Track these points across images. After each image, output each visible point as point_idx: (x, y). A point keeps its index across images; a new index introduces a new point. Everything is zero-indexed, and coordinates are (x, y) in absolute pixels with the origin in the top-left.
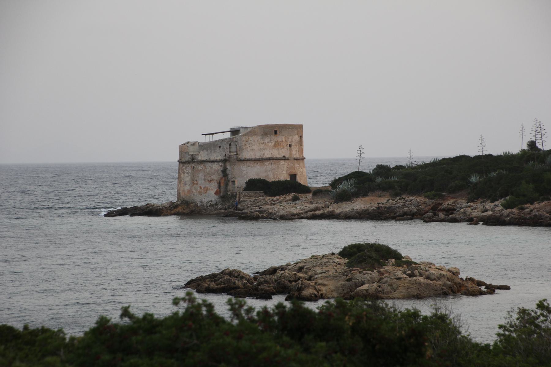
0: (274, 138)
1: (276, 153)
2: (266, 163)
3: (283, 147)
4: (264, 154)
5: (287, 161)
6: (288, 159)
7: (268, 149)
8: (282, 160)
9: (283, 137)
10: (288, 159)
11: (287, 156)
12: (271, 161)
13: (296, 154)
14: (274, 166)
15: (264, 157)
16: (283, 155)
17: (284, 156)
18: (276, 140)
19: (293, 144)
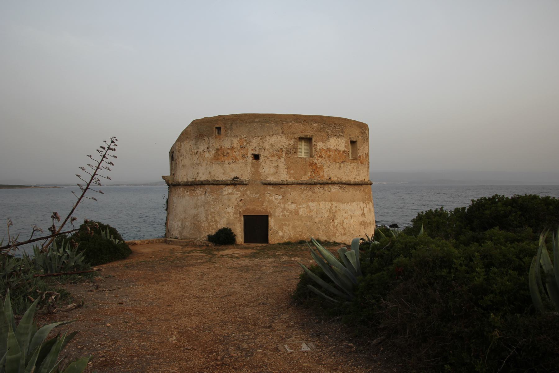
0: (215, 143)
1: (220, 172)
3: (235, 160)
4: (198, 173)
5: (241, 188)
6: (242, 184)
8: (228, 185)
10: (242, 184)
11: (245, 178)
12: (206, 187)
13: (275, 174)
14: (210, 198)
15: (198, 179)
16: (233, 175)
17: (236, 178)
18: (217, 146)
19: (262, 155)
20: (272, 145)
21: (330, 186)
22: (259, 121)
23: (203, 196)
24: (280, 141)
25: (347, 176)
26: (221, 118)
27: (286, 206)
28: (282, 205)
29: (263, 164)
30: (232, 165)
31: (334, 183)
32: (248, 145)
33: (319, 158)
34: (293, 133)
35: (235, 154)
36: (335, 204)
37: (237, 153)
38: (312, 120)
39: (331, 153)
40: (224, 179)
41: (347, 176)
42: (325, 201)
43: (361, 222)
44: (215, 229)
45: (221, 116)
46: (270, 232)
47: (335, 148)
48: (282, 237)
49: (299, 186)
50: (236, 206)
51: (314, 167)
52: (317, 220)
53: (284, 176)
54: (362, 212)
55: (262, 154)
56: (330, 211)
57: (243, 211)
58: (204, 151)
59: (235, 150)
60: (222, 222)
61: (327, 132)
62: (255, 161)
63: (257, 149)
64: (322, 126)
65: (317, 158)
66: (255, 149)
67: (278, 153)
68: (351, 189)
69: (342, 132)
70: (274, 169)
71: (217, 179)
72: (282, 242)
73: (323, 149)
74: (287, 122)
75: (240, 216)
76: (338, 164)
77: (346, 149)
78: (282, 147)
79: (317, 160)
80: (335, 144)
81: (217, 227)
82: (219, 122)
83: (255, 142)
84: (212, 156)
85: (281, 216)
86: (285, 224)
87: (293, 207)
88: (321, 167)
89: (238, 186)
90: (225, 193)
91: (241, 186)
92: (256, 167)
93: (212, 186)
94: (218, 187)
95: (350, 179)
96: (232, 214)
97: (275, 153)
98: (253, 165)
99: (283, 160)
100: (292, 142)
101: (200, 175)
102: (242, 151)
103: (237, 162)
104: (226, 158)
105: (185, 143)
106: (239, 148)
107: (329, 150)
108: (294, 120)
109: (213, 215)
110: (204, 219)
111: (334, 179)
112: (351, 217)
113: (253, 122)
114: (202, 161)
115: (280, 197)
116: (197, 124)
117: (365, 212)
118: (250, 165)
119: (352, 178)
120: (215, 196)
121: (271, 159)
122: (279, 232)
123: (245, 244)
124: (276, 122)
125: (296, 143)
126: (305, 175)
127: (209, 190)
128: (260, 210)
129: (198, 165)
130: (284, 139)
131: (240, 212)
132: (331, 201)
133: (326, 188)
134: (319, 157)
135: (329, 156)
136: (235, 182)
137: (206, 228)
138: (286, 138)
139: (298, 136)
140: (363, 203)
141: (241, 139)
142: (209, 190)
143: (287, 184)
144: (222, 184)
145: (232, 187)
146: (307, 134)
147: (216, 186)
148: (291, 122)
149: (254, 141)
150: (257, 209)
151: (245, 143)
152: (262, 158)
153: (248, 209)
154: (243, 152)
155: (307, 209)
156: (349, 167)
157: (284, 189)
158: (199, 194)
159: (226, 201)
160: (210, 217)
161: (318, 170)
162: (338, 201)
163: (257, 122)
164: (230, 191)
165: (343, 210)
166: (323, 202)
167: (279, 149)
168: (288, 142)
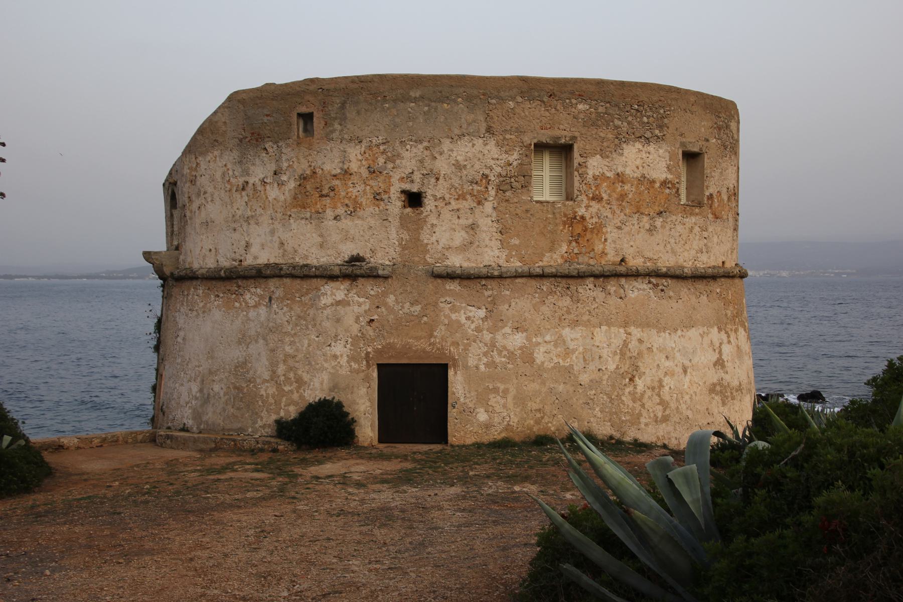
2: (252, 294)
4: (248, 246)
5: (372, 288)
6: (373, 275)
7: (265, 219)
8: (332, 278)
9: (354, 153)
10: (373, 275)
11: (382, 259)
12: (272, 283)
13: (465, 247)
14: (282, 315)
15: (249, 261)
16: (348, 250)
17: (356, 259)
18: (303, 167)
19: (432, 193)
20: (459, 167)
21: (623, 281)
22: (422, 97)
23: (263, 310)
24: (483, 154)
25: (674, 252)
26: (312, 87)
27: (499, 337)
28: (487, 336)
29: (432, 220)
30: (346, 223)
31: (635, 275)
32: (390, 165)
33: (593, 203)
34: (519, 131)
35: (354, 192)
36: (636, 332)
37: (360, 187)
38: (572, 93)
39: (627, 187)
40: (324, 260)
41: (674, 252)
42: (609, 324)
43: (714, 385)
44: (295, 403)
45: (312, 81)
46: (452, 413)
47: (638, 174)
48: (487, 426)
49: (533, 283)
50: (355, 339)
51: (578, 229)
52: (584, 378)
53: (491, 254)
54: (715, 357)
55: (429, 192)
56: (623, 354)
57: (377, 351)
58: (263, 182)
59: (355, 179)
60: (316, 383)
61: (617, 127)
62: (409, 210)
63: (417, 177)
64: (601, 109)
65: (585, 201)
66: (409, 178)
67: (476, 187)
68: (684, 290)
69: (661, 127)
70: (463, 233)
71: (302, 262)
72: (486, 439)
73: (603, 178)
74: (502, 100)
75: (368, 366)
76: (645, 219)
77: (670, 177)
78: (487, 172)
79: (587, 207)
80: (639, 162)
81: (301, 397)
82: (308, 97)
83: (410, 159)
84: (288, 196)
85: (482, 367)
86: (496, 390)
87: (518, 340)
88: (598, 229)
89: (361, 281)
90: (325, 301)
91: (371, 281)
92: (413, 227)
93: (287, 281)
94: (306, 284)
95: (681, 261)
96: (344, 361)
97: (468, 187)
98: (404, 222)
99: (488, 207)
100: (514, 157)
101: (254, 250)
102: (371, 183)
103: (360, 213)
104: (327, 201)
105: (210, 157)
106: (365, 173)
107: (620, 178)
108: (522, 94)
109: (291, 362)
110: (266, 375)
111: (636, 262)
112: (685, 371)
113: (406, 99)
114: (259, 211)
115: (482, 313)
116: (242, 102)
117: (724, 357)
118: (395, 222)
119: (687, 257)
120: (297, 309)
121: (454, 205)
122: (478, 410)
123: (382, 446)
124: (469, 99)
125: (526, 160)
126: (552, 249)
127: (279, 293)
128: (424, 351)
129: (247, 220)
130: (491, 150)
131: (368, 354)
132: (625, 325)
133: (612, 286)
134: (593, 199)
135: (622, 197)
136: (354, 271)
137: (271, 400)
138: (497, 144)
139: (530, 139)
140: (720, 330)
141: (370, 148)
142: (279, 293)
143: (500, 277)
144: (316, 277)
145: (347, 284)
146: (557, 133)
147: (298, 281)
148: (513, 98)
149: (406, 155)
150: (417, 348)
151: (381, 161)
152: (429, 204)
153: (390, 346)
154: (377, 184)
155: (556, 346)
156: (679, 228)
157: (491, 290)
158: (252, 303)
159: (327, 324)
160: (281, 369)
161: (588, 236)
162: (645, 325)
163: (415, 100)
164: (340, 295)
165: (661, 350)
166: (604, 328)
167: (478, 178)
168: (504, 156)
